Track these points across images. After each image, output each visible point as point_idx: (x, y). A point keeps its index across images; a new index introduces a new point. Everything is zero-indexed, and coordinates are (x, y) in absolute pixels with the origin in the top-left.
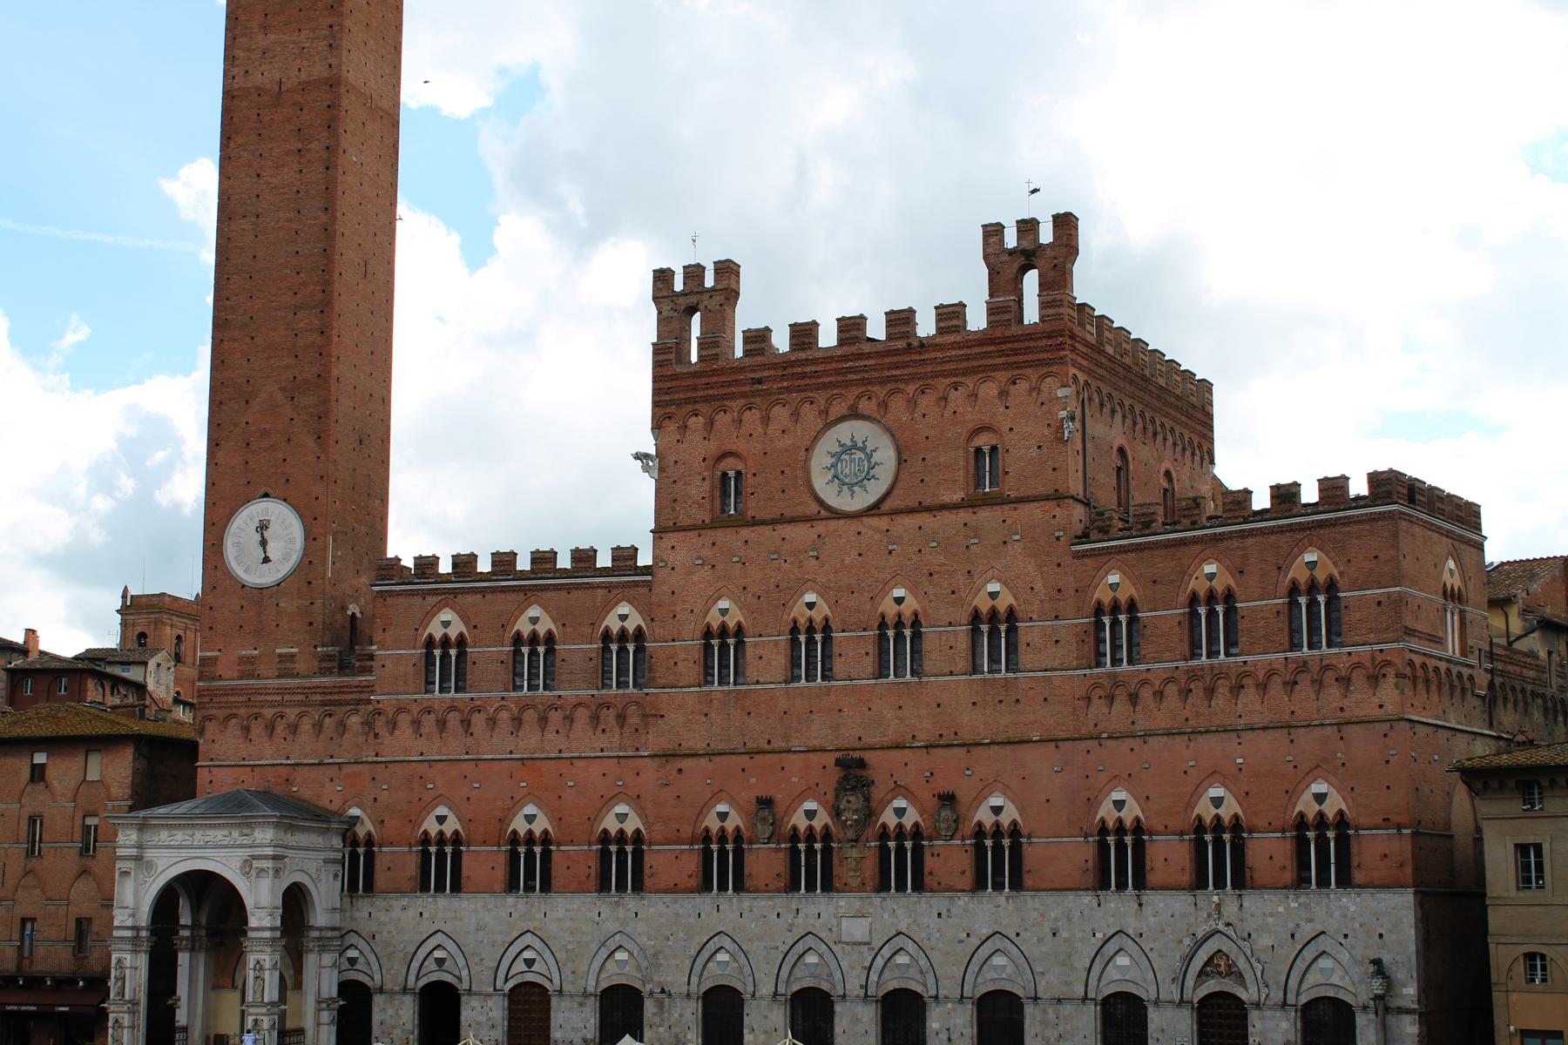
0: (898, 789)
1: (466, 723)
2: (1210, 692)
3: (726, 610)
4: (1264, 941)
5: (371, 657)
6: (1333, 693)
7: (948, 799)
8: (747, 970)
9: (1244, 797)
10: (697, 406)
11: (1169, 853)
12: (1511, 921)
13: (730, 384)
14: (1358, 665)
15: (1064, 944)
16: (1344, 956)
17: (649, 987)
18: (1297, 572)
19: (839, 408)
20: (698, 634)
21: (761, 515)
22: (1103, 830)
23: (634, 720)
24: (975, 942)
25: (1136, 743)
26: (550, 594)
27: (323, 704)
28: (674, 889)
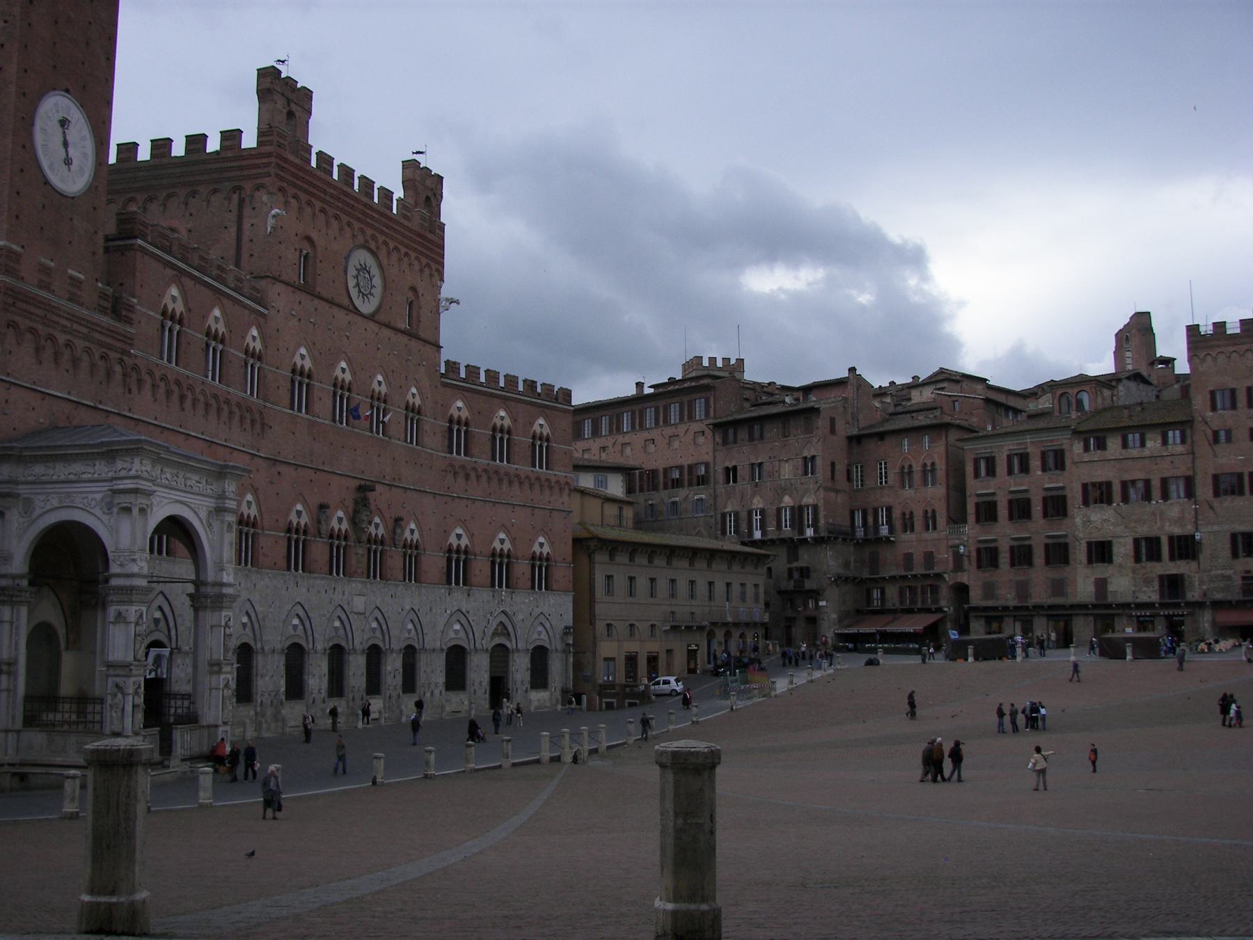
0: (381, 513)
1: (182, 398)
2: (500, 480)
3: (303, 358)
4: (520, 617)
5: (131, 308)
6: (547, 492)
7: (398, 521)
8: (309, 632)
9: (513, 541)
10: (299, 193)
11: (480, 567)
12: (605, 609)
13: (315, 187)
14: (558, 482)
15: (437, 615)
16: (548, 626)
17: (259, 646)
18: (536, 428)
19: (361, 239)
20: (290, 369)
21: (324, 294)
22: (450, 550)
23: (258, 426)
24: (404, 613)
25: (469, 503)
26: (225, 301)
27: (102, 344)
28: (274, 566)
